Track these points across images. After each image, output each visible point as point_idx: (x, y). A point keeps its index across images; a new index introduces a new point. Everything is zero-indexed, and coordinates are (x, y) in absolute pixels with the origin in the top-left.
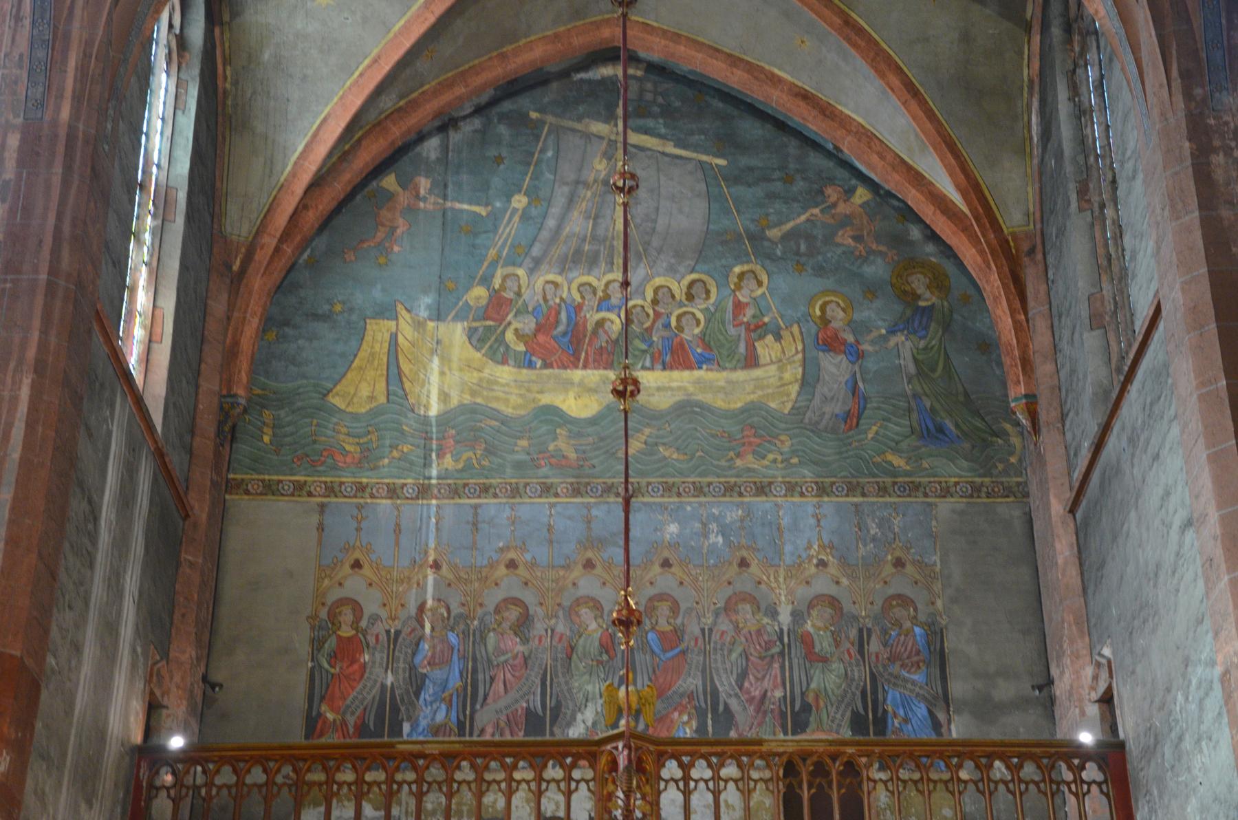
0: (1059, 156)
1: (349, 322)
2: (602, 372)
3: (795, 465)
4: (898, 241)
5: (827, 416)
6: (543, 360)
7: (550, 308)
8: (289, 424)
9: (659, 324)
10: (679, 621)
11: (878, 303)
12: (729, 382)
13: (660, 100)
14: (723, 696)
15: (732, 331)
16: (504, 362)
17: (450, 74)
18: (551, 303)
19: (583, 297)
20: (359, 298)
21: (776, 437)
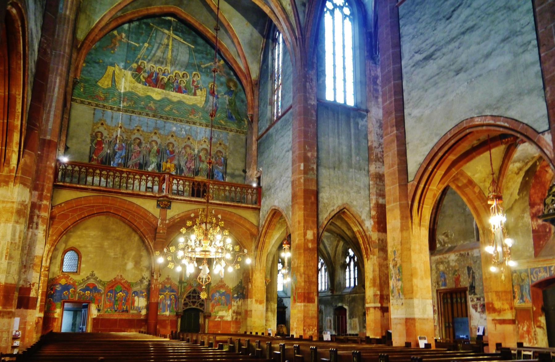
0: (267, 66)
1: (103, 65)
4: (228, 74)
8: (88, 87)
9: (176, 81)
10: (174, 149)
11: (223, 87)
13: (181, 28)
14: (182, 166)
15: (192, 87)
16: (140, 83)
17: (134, 10)
20: (106, 60)
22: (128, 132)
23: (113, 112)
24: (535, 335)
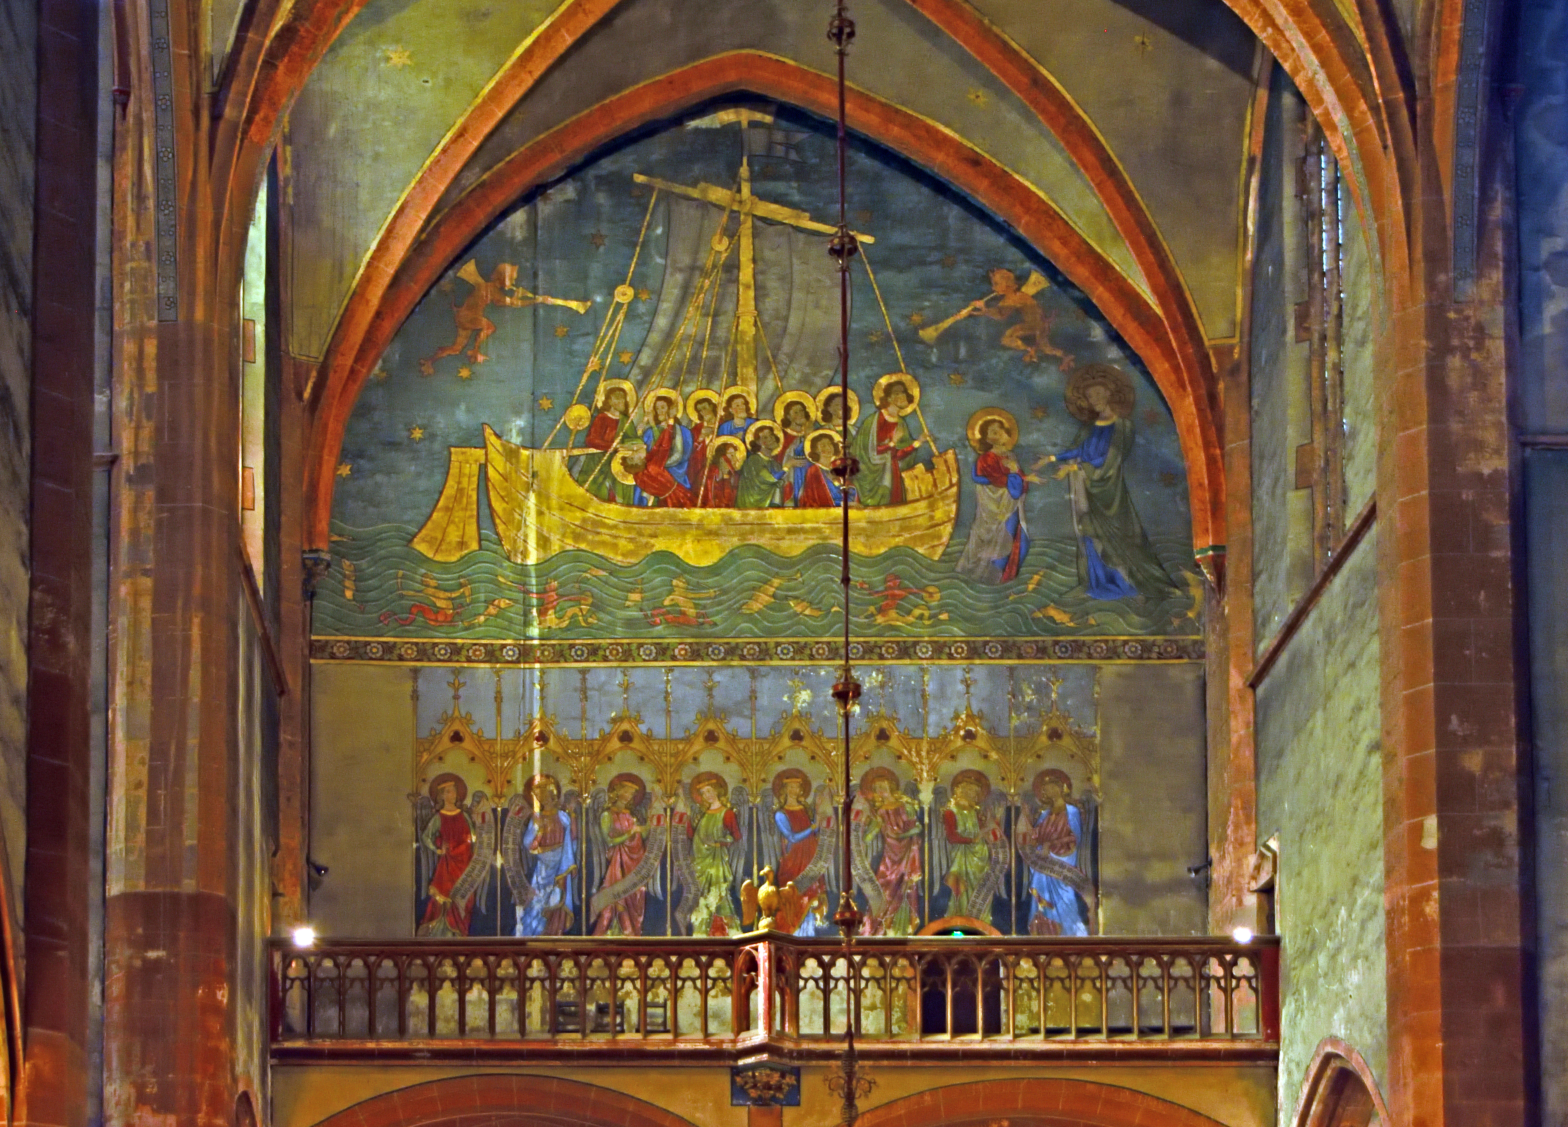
2: (723, 510)
3: (942, 622)
5: (983, 563)
6: (656, 496)
7: (663, 431)
12: (871, 522)
15: (876, 459)
18: (664, 425)
19: (701, 418)
21: (923, 589)
22: (576, 756)
23: (497, 672)
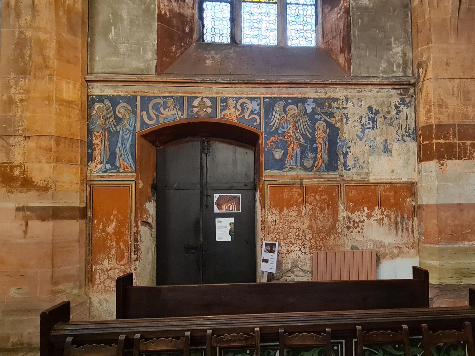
24: (136, 240)
